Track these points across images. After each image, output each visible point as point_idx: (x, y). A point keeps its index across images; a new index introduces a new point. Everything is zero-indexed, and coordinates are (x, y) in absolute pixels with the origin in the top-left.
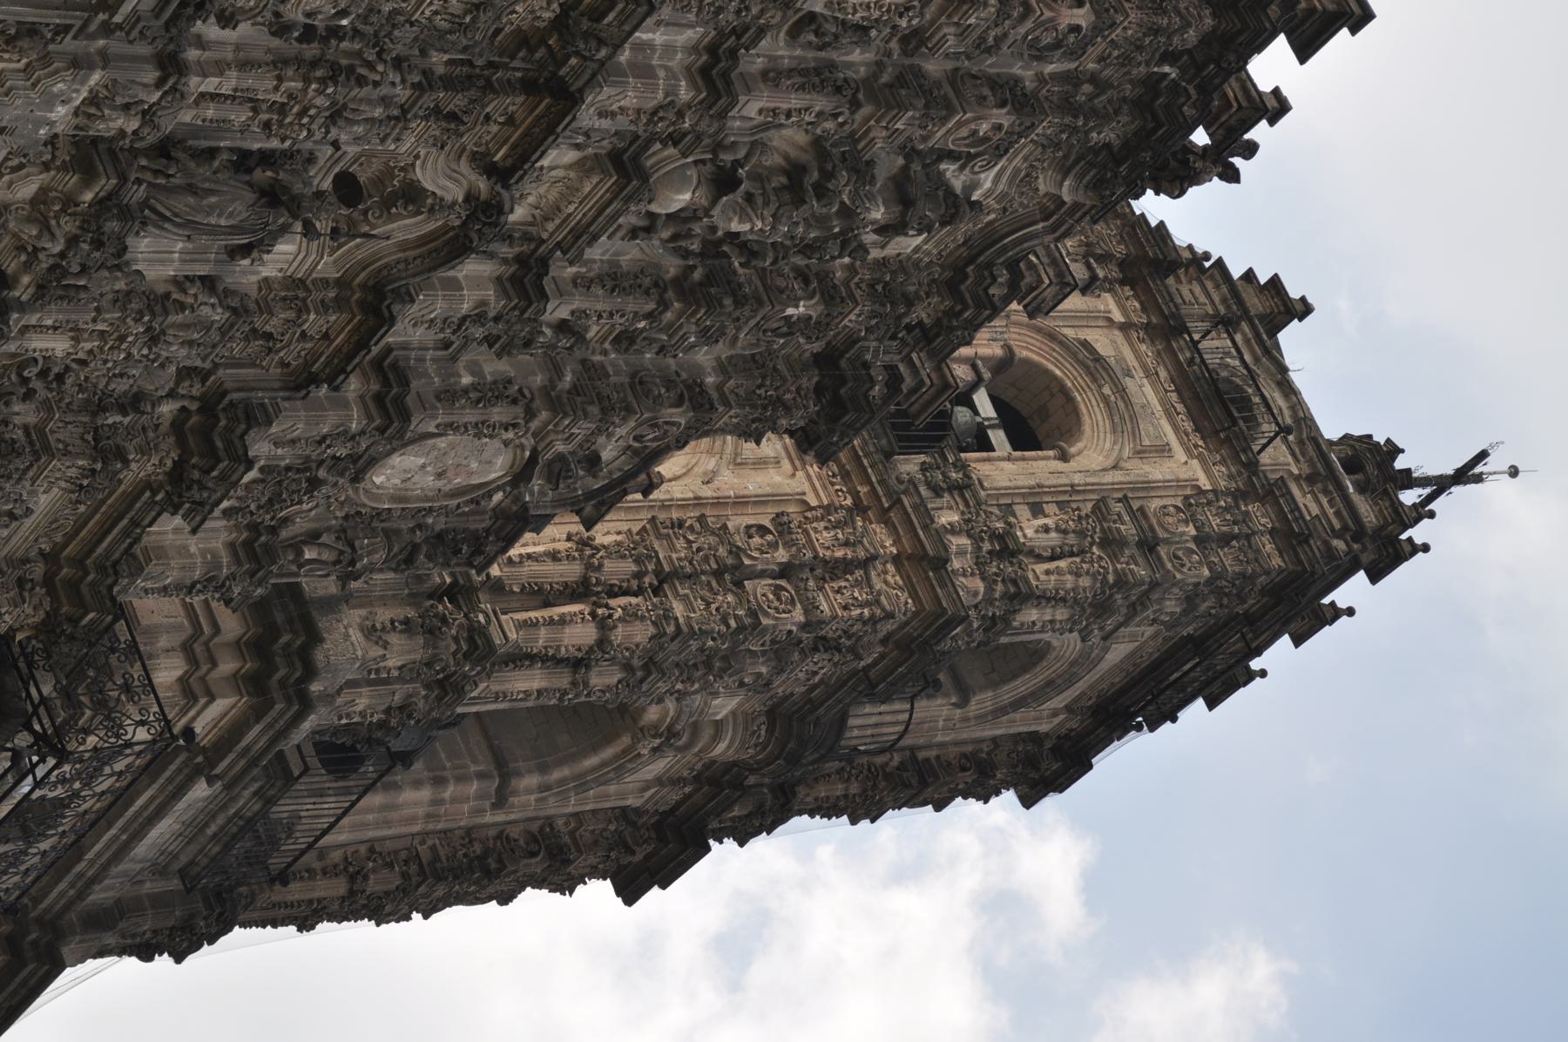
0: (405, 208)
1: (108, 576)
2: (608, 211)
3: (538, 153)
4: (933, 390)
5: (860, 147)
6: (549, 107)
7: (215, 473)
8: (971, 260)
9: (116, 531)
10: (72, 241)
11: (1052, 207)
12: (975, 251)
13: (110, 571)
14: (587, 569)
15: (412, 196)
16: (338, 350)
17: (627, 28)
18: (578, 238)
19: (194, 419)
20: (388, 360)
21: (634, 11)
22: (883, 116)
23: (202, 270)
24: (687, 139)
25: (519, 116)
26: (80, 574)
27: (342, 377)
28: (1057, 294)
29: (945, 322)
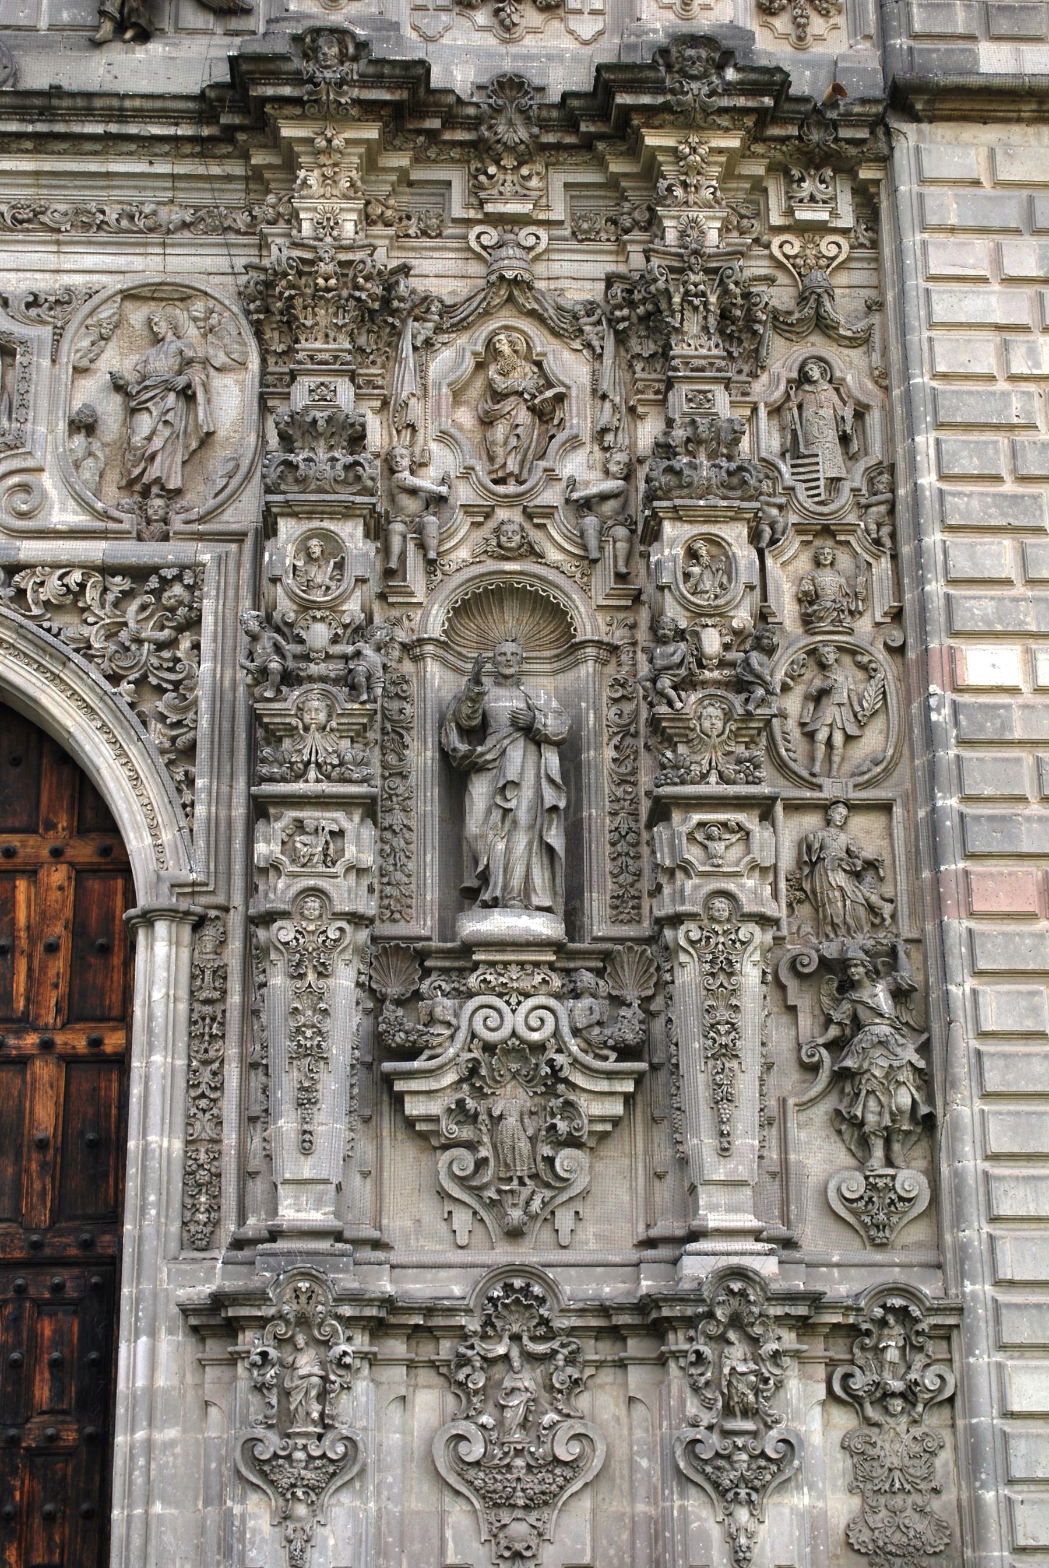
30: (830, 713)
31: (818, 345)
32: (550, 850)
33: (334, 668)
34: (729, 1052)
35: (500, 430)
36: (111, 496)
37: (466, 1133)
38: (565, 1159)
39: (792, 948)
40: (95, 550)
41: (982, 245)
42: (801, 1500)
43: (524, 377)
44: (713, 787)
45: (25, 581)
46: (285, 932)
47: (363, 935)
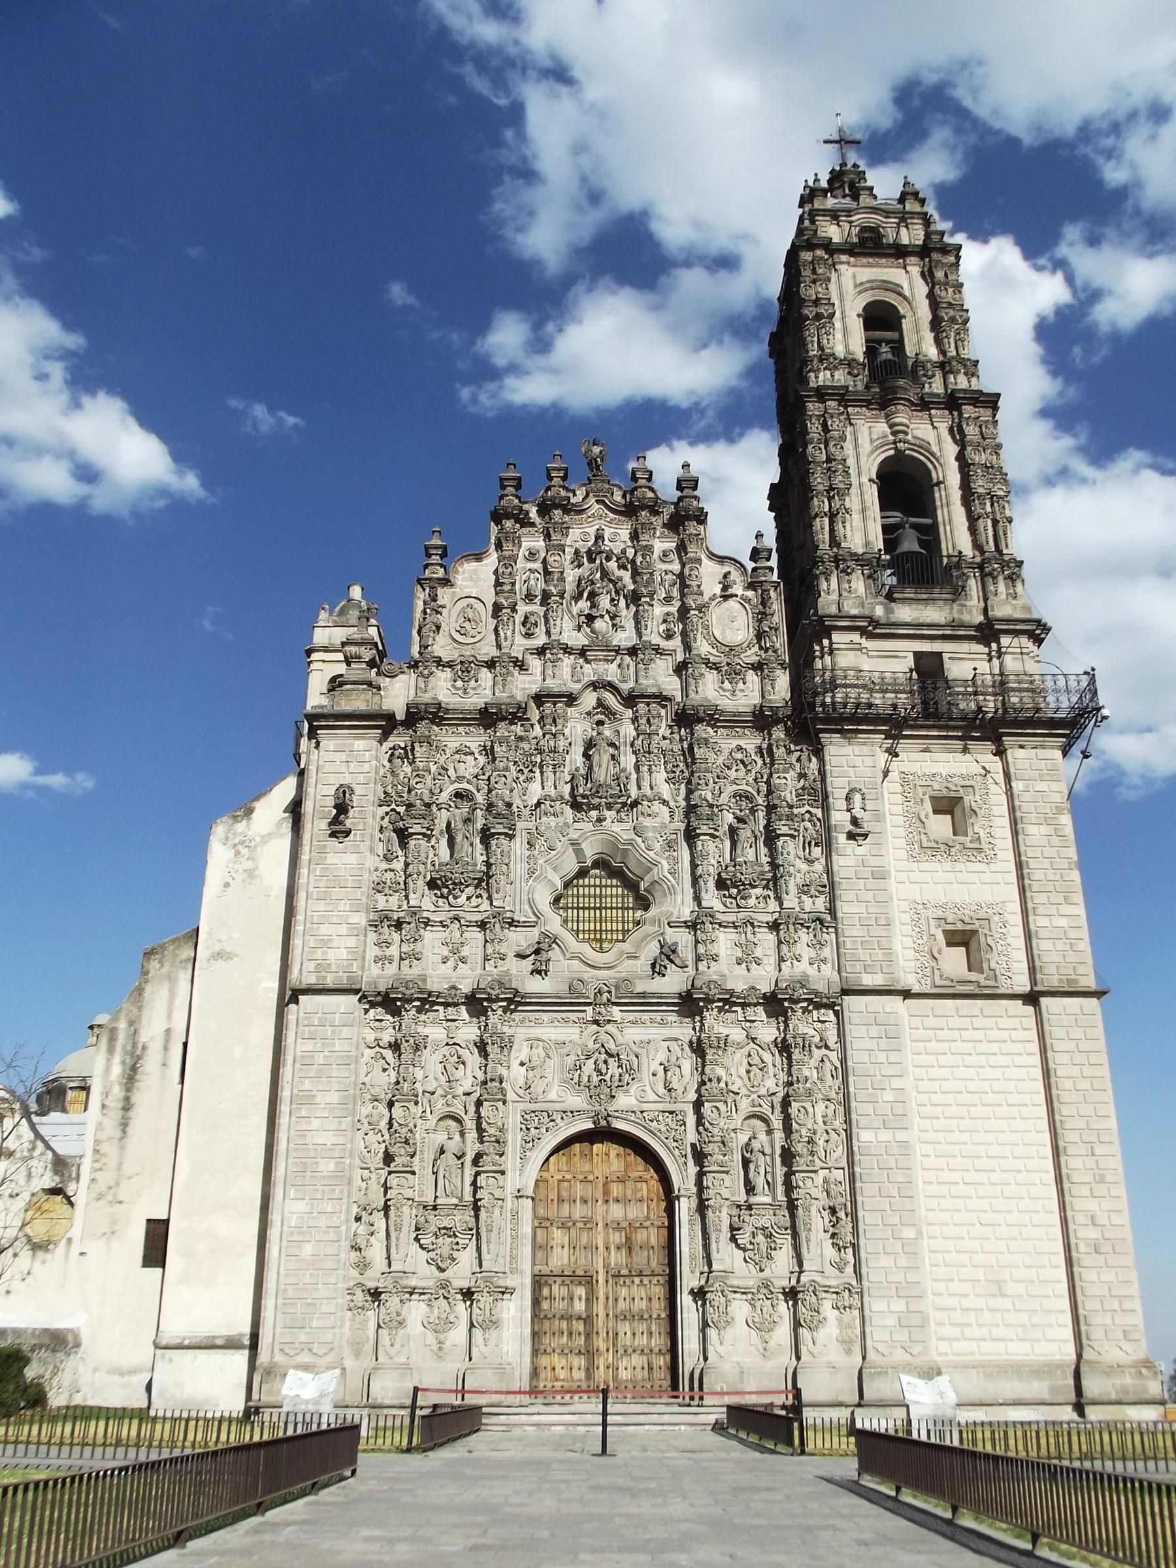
10: (600, 798)
15: (600, 703)
23: (629, 749)
30: (831, 1145)
31: (824, 1051)
32: (768, 1182)
33: (719, 1139)
34: (810, 1230)
35: (752, 1074)
36: (662, 1091)
37: (751, 1247)
38: (773, 1253)
39: (823, 1202)
40: (661, 1107)
41: (865, 1028)
42: (828, 1330)
43: (756, 1060)
44: (805, 1168)
45: (645, 1114)
46: (711, 1203)
47: (728, 1203)
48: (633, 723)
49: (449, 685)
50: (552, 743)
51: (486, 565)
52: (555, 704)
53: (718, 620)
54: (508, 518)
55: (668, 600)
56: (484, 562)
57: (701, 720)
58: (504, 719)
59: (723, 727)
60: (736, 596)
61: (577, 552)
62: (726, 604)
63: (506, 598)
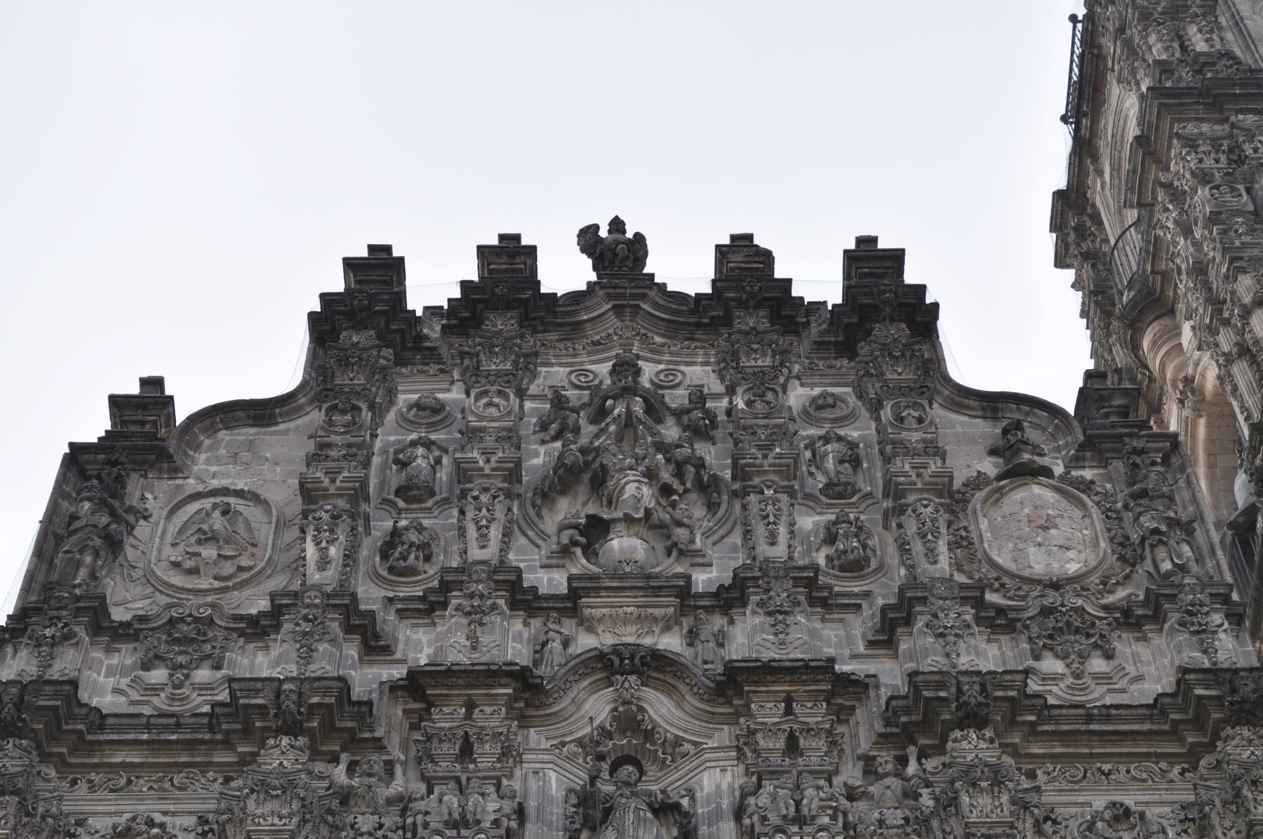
0: (643, 720)
1: (1162, 705)
2: (614, 585)
3: (477, 668)
4: (862, 265)
5: (512, 465)
6: (436, 687)
7: (942, 694)
8: (699, 325)
9: (1111, 728)
11: (628, 310)
12: (690, 328)
13: (1159, 706)
14: (1233, 361)
16: (792, 682)
17: (259, 685)
18: (660, 588)
19: (923, 741)
20: (881, 638)
21: (241, 690)
22: (474, 470)
24: (501, 578)
25: (461, 701)
26: (1181, 727)
27: (812, 664)
28: (734, 252)
29: (752, 303)
48: (741, 756)
49: (124, 682)
50: (453, 801)
51: (286, 432)
52: (470, 706)
53: (994, 529)
54: (360, 326)
55: (837, 490)
56: (282, 427)
57: (973, 718)
58: (293, 729)
59: (1053, 757)
60: (1047, 472)
61: (559, 401)
62: (1018, 495)
63: (332, 474)
